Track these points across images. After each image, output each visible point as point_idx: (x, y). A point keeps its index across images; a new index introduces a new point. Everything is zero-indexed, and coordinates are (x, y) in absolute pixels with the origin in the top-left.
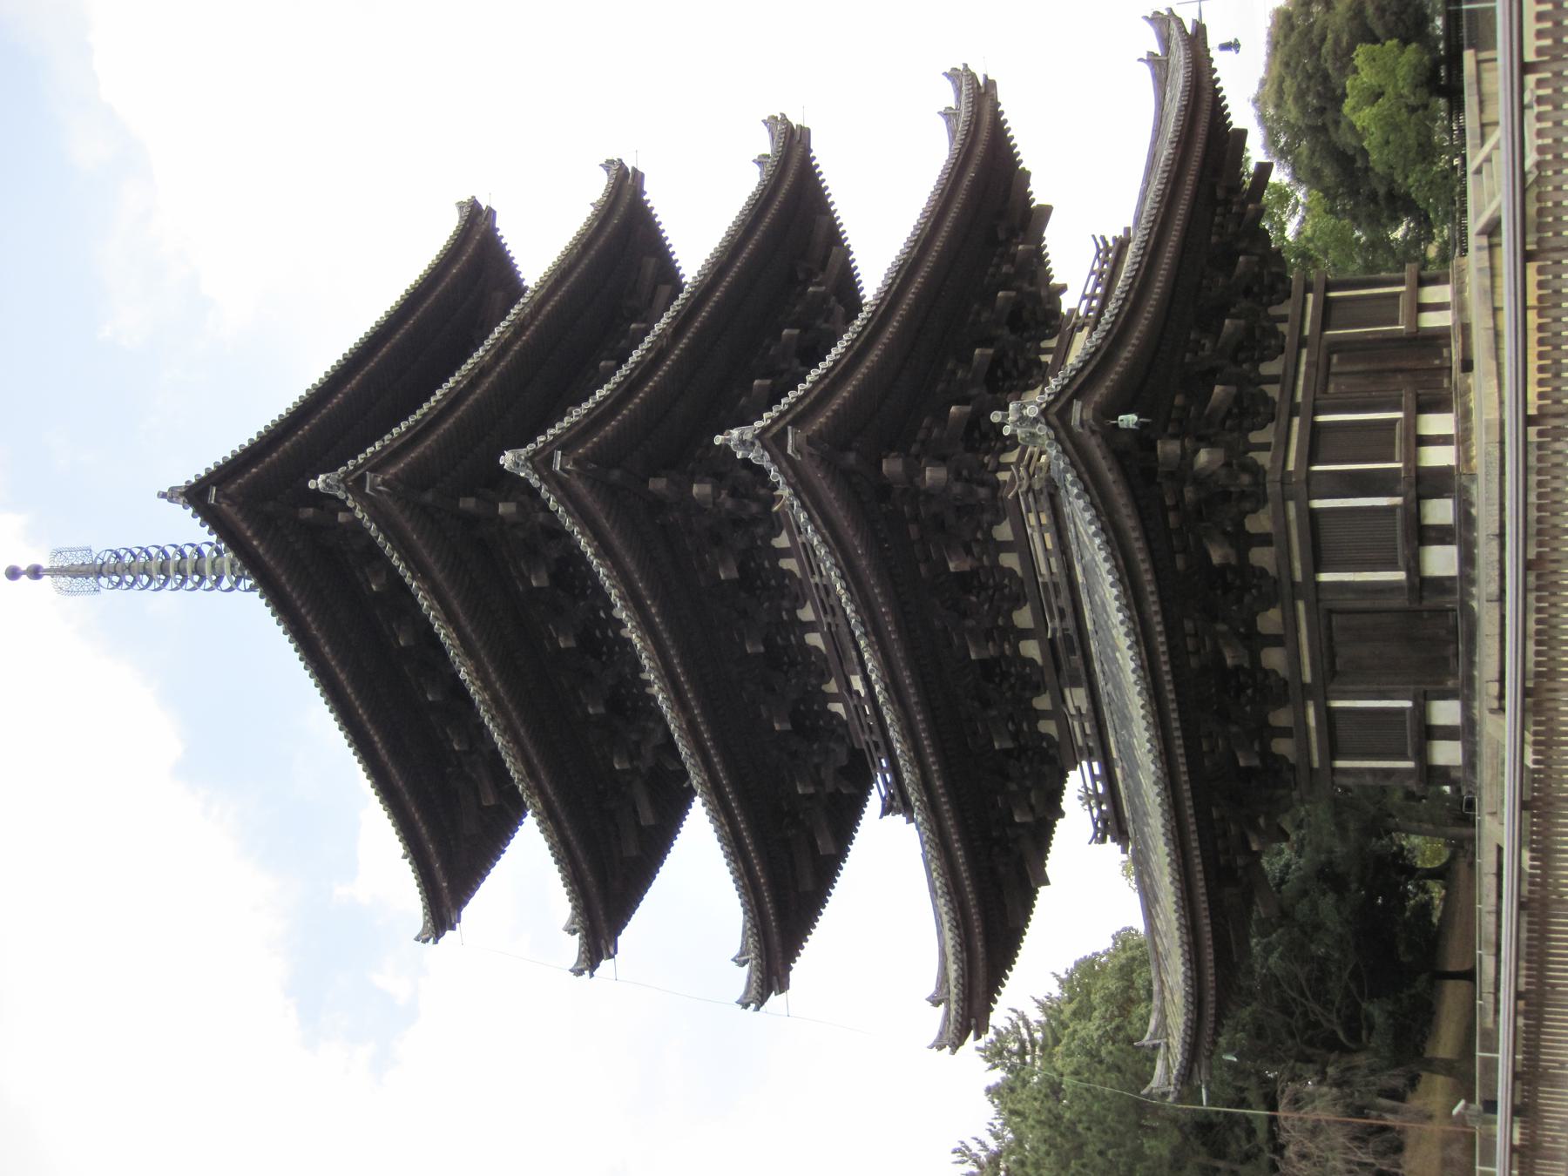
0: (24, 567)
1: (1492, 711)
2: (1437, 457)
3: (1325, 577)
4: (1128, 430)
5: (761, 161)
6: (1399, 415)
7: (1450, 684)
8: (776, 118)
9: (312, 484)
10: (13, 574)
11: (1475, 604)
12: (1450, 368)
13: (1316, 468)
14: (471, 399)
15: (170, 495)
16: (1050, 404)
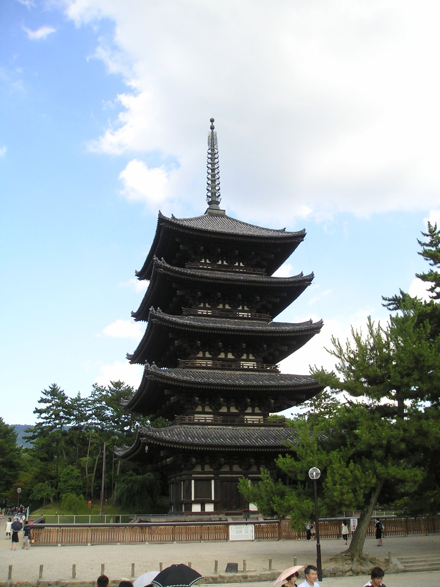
0: (213, 123)
1: (140, 519)
2: (196, 508)
3: (182, 482)
4: (145, 448)
5: (311, 321)
6: (213, 499)
7: (175, 510)
8: (322, 322)
9: (155, 256)
10: (212, 121)
11: (178, 515)
12: (231, 510)
13: (193, 481)
14: (196, 279)
15: (160, 214)
16: (142, 433)
